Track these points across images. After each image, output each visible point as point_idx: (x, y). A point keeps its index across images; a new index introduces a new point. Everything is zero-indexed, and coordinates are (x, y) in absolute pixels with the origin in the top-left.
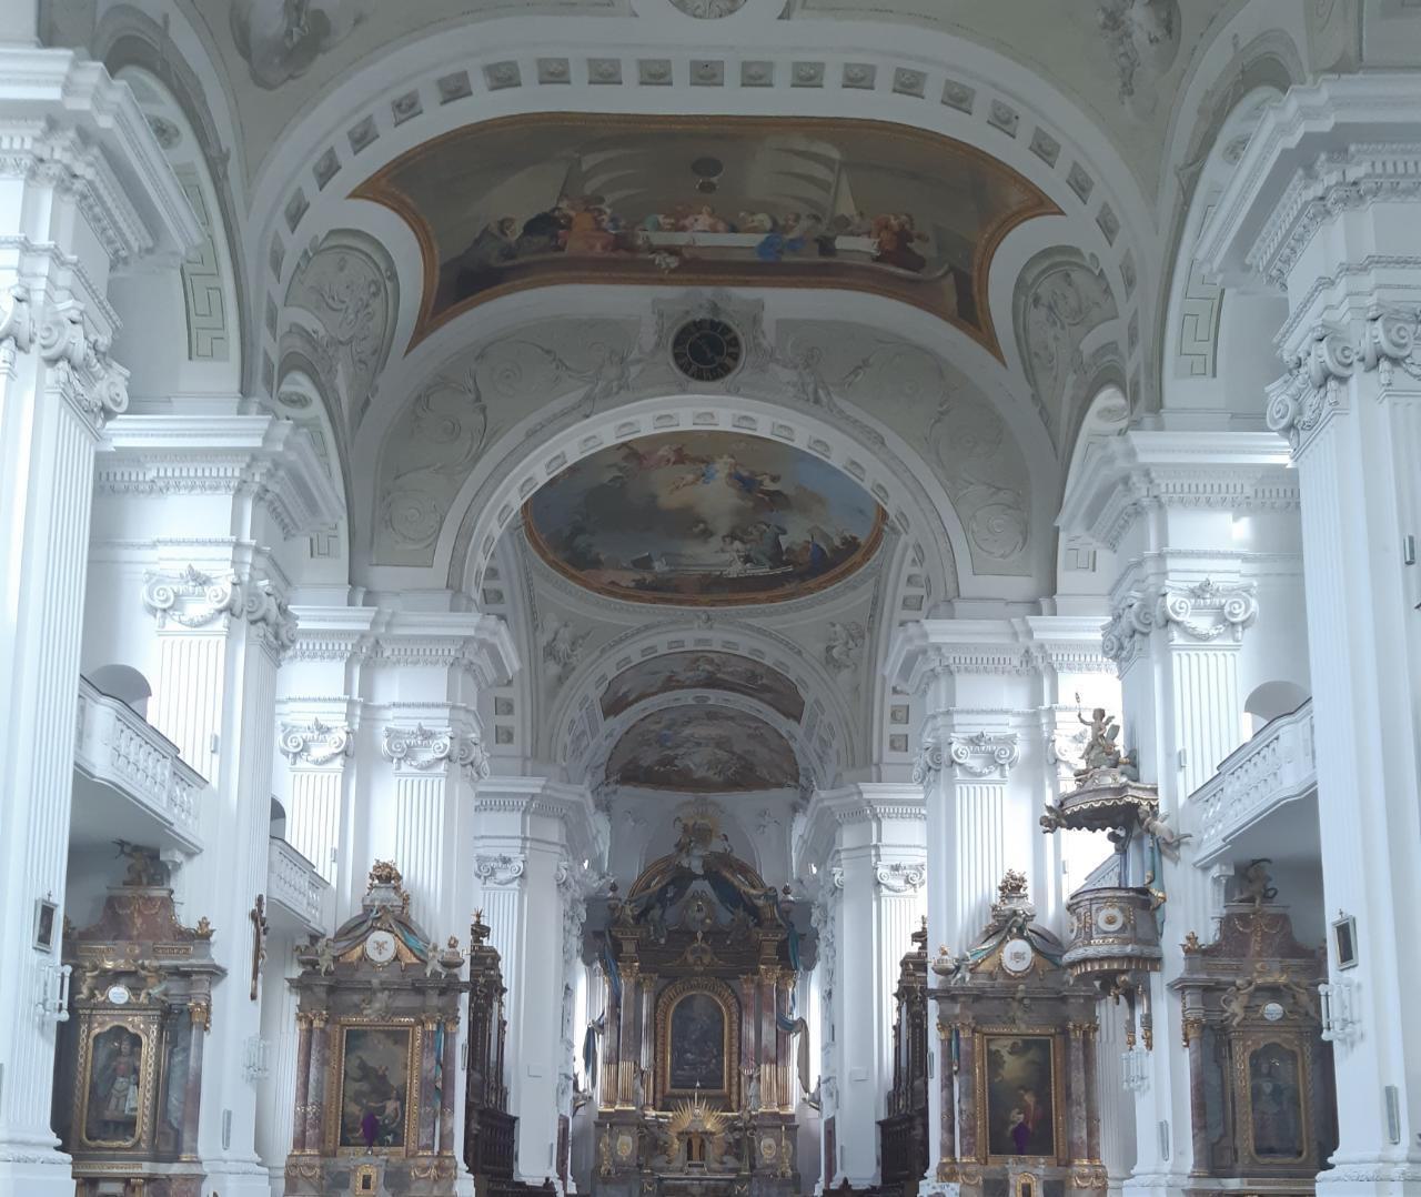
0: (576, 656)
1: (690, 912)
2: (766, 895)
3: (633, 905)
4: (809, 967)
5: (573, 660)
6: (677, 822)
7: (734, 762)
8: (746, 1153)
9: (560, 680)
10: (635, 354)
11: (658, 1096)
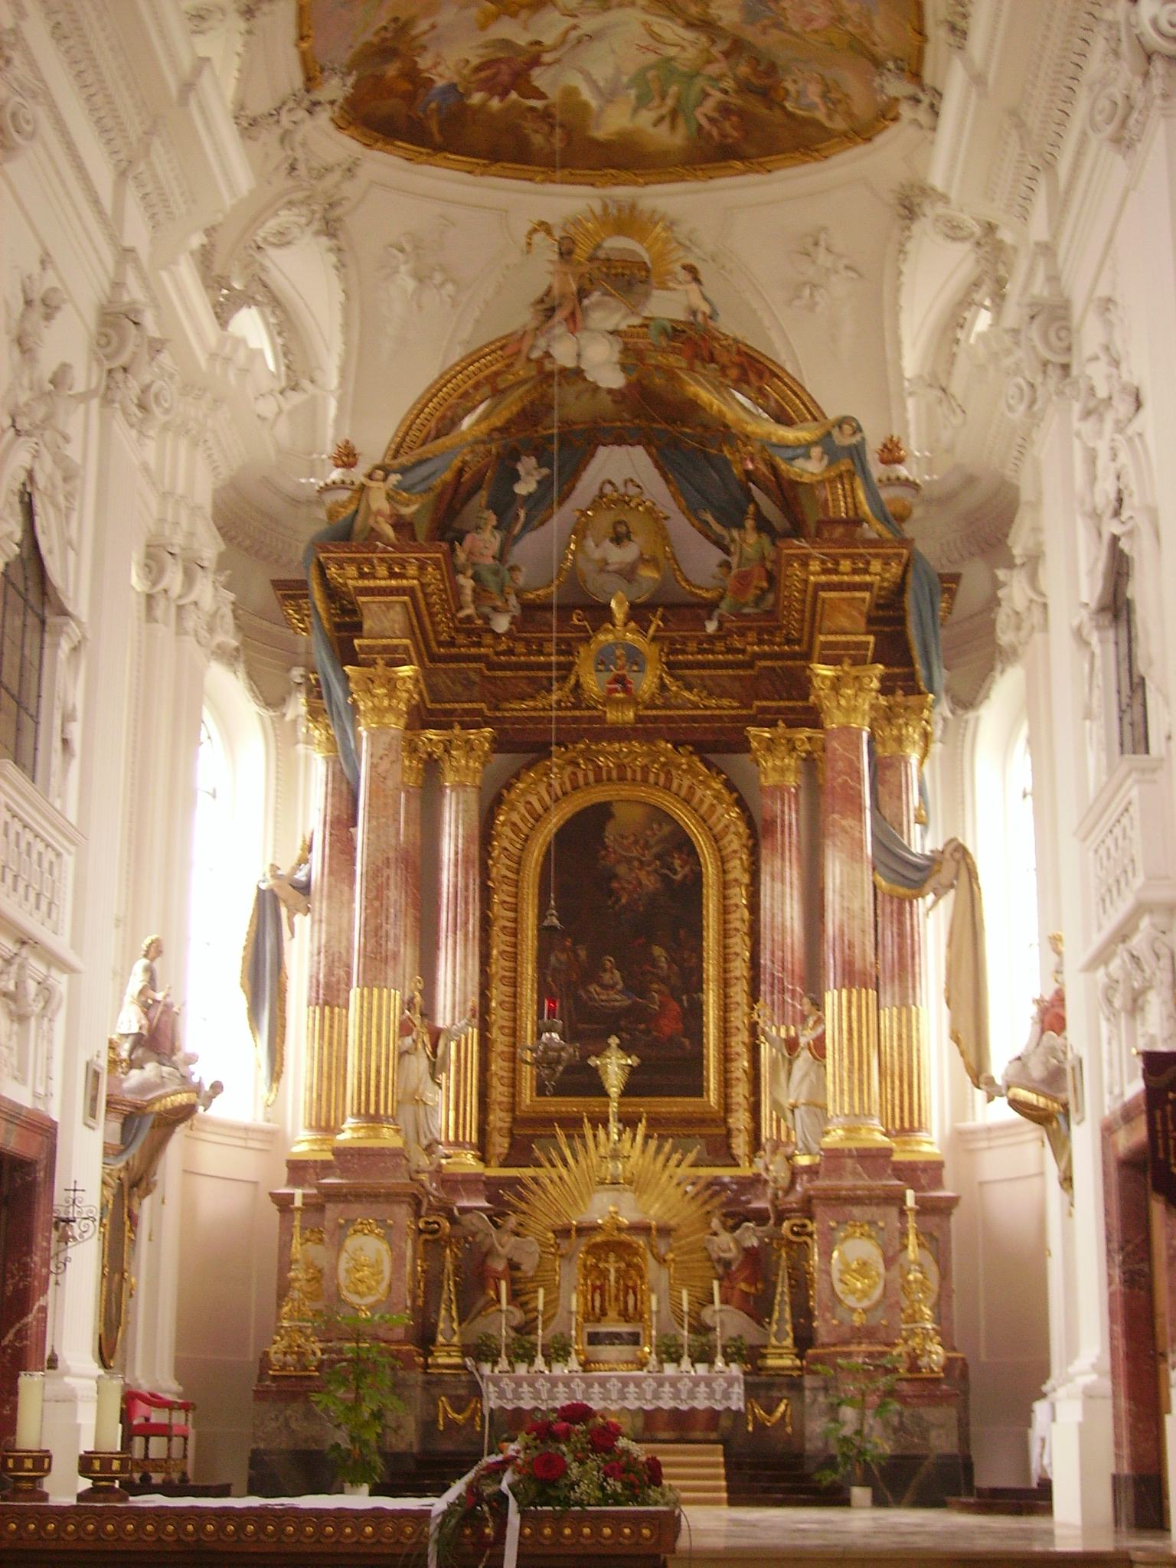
1: (590, 543)
2: (833, 453)
3: (394, 478)
4: (967, 701)
6: (539, 237)
7: (714, 69)
8: (782, 1289)
11: (499, 1118)
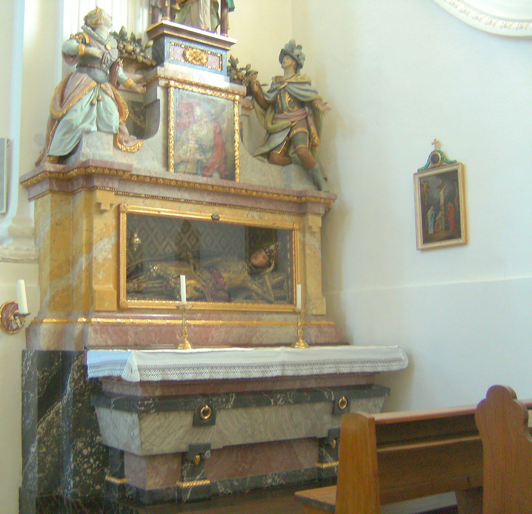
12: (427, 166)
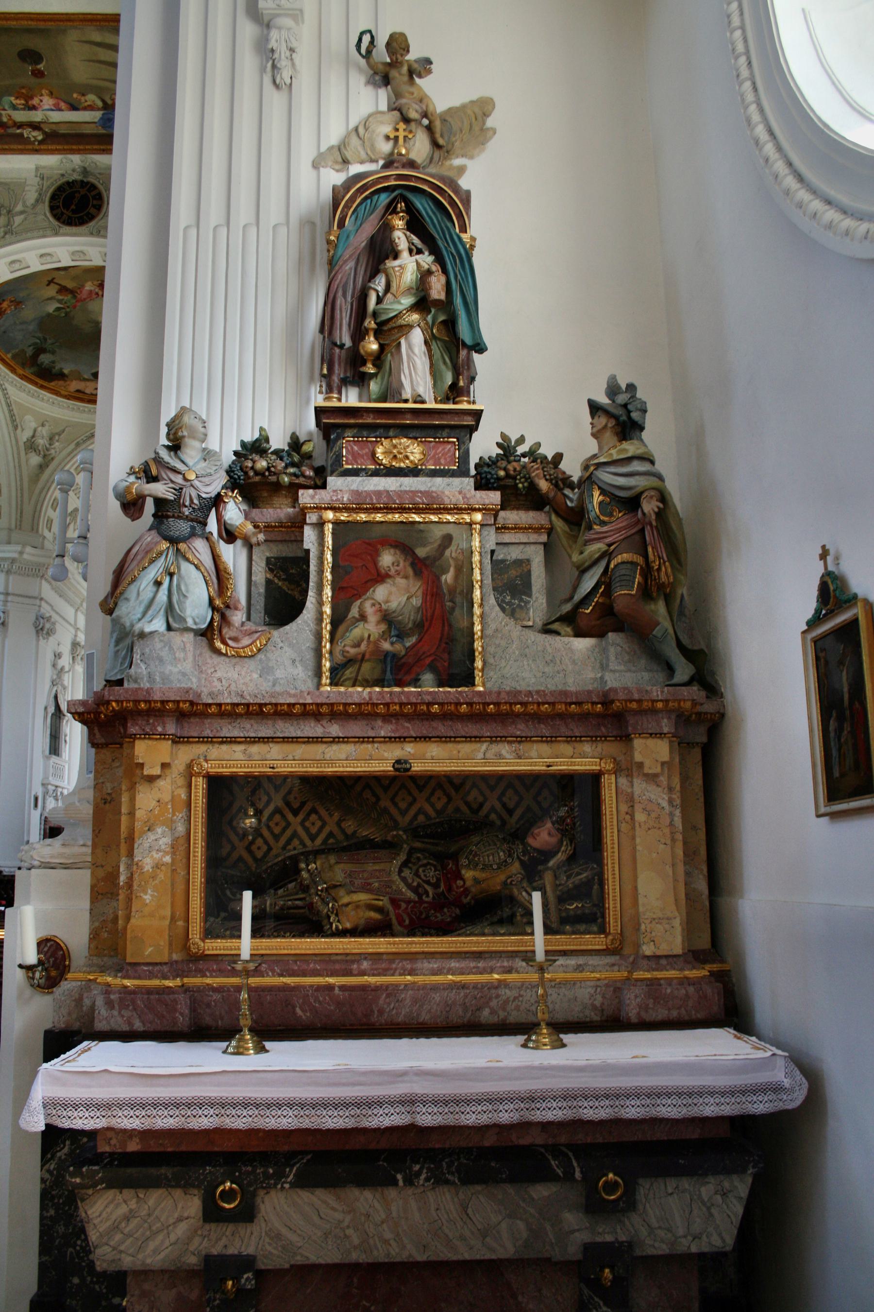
0: (54, 448)
5: (53, 451)
9: (42, 467)
10: (20, 207)
12: (818, 611)
